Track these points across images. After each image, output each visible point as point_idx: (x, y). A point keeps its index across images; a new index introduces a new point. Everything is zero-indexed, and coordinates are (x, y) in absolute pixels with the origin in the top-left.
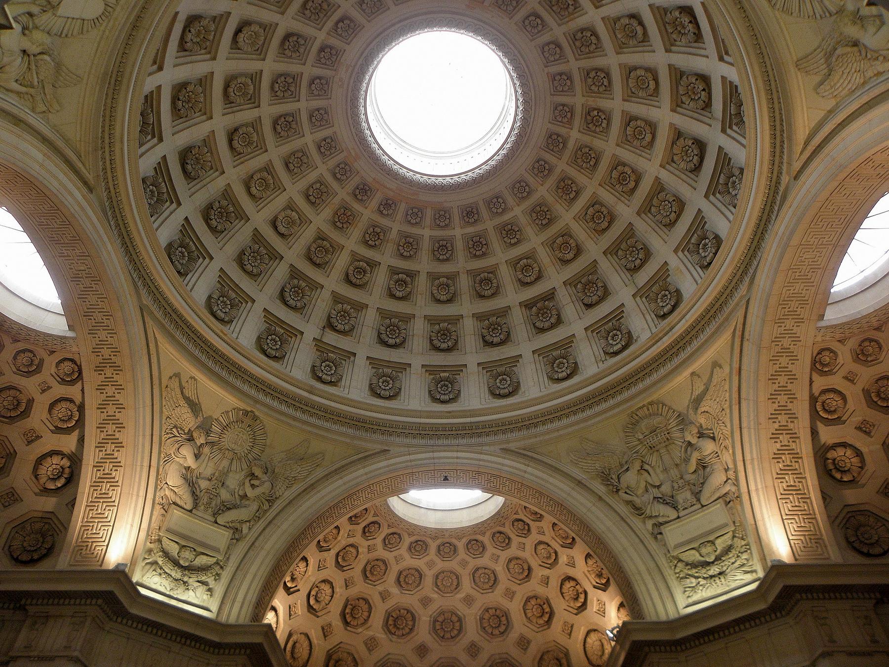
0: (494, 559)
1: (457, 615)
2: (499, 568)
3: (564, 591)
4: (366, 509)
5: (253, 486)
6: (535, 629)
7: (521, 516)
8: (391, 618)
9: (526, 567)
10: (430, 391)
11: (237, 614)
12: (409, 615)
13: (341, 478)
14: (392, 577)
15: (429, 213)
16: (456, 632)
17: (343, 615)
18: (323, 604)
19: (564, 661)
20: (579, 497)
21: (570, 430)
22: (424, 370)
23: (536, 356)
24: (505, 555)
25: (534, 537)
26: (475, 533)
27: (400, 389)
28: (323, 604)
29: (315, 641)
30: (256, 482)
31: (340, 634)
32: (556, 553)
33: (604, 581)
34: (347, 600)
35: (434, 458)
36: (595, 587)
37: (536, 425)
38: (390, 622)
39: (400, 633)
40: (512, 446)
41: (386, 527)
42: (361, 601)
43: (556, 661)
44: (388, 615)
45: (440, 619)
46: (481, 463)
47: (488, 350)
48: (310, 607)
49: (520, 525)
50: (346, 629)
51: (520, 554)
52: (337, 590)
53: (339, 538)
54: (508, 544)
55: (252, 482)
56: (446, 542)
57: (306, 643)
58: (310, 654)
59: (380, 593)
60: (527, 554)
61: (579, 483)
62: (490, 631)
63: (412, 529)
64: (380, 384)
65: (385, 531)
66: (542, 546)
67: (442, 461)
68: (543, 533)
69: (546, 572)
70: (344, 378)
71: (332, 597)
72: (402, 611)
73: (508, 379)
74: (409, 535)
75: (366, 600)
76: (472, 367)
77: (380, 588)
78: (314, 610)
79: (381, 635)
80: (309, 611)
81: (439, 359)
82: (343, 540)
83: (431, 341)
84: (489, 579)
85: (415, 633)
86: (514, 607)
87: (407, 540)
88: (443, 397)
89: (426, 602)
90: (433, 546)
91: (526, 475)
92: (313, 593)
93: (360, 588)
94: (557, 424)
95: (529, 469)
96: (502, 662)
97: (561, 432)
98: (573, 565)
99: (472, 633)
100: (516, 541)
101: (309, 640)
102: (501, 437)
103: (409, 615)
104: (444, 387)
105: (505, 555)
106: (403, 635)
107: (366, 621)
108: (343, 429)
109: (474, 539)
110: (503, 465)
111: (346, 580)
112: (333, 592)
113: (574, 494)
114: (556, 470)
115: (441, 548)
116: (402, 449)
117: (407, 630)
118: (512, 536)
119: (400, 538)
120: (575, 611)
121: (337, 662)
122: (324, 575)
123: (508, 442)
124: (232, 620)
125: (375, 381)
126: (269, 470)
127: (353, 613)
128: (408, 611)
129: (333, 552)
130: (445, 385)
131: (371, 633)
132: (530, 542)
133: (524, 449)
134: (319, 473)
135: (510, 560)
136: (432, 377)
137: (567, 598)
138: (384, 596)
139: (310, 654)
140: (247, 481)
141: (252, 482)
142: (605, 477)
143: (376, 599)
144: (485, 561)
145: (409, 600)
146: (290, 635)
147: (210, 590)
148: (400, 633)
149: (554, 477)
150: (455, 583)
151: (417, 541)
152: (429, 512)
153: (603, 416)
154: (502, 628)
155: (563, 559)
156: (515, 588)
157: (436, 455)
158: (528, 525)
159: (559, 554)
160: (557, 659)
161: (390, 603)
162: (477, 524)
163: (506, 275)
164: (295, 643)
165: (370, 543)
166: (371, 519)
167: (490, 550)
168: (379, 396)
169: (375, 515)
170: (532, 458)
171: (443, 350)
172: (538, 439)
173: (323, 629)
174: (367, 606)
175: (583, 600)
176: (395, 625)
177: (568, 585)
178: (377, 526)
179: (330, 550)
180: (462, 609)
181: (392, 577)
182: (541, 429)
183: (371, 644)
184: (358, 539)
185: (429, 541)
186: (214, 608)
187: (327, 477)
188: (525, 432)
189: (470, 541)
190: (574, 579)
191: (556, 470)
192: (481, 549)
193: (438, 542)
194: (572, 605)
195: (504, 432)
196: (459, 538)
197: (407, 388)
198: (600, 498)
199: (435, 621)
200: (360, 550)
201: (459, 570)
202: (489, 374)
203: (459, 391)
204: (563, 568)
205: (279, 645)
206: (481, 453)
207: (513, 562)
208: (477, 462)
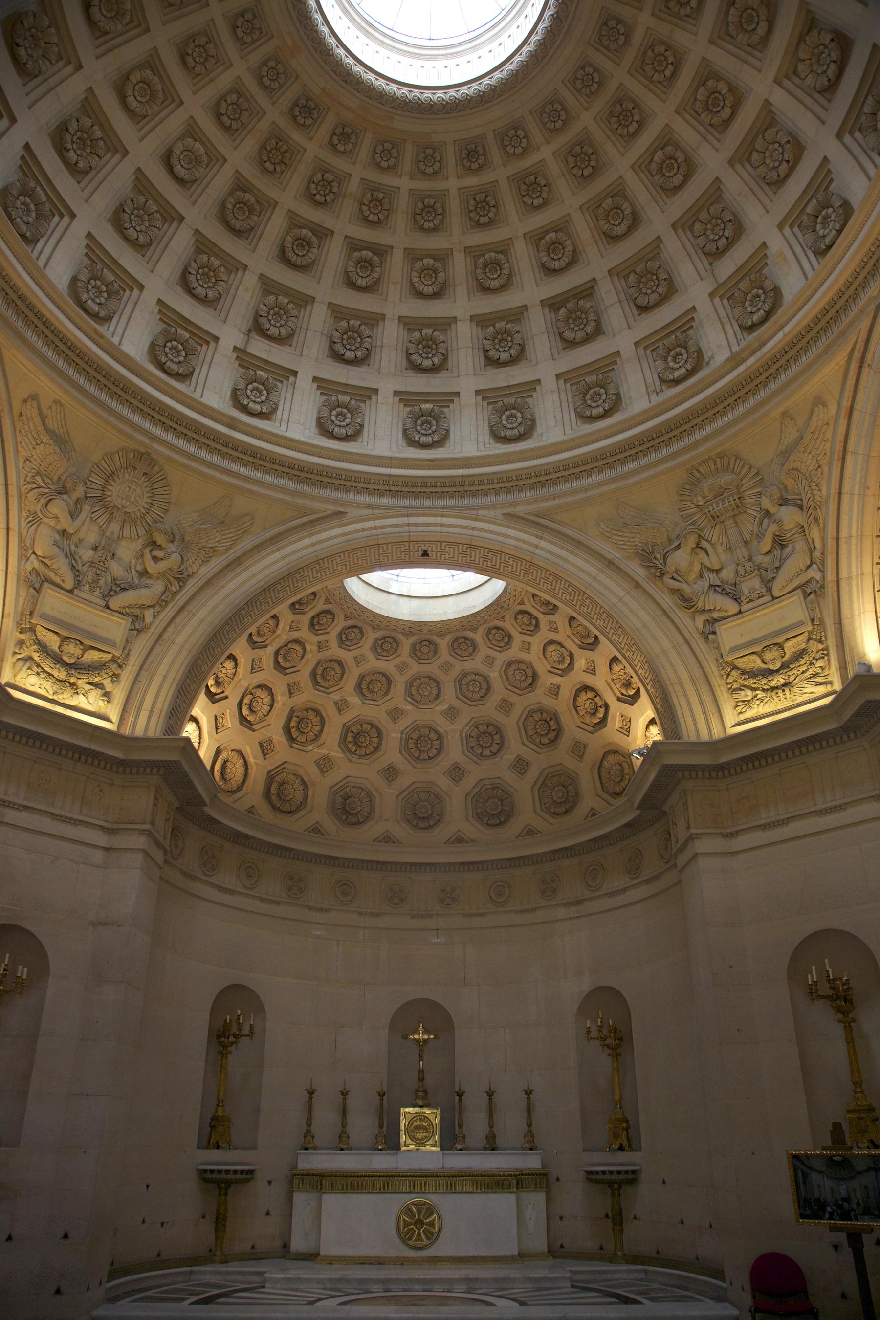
0: (489, 662)
1: (436, 732)
2: (494, 675)
3: (579, 704)
4: (314, 594)
5: (155, 559)
7: (528, 607)
8: (350, 734)
9: (530, 674)
10: (405, 431)
12: (374, 730)
13: (278, 550)
14: (350, 682)
15: (409, 151)
16: (434, 752)
17: (287, 729)
18: (260, 714)
20: (608, 582)
21: (604, 489)
22: (397, 399)
23: (561, 382)
24: (501, 658)
25: (544, 635)
26: (464, 628)
27: (362, 426)
28: (260, 714)
29: (251, 760)
30: (159, 554)
31: (283, 752)
32: (571, 656)
33: (632, 692)
34: (292, 711)
35: (408, 525)
36: (619, 699)
37: (555, 482)
38: (349, 739)
39: (363, 752)
40: (520, 510)
41: (342, 617)
42: (310, 712)
43: (561, 788)
44: (347, 729)
45: (415, 736)
46: (476, 533)
47: (492, 371)
48: (243, 719)
49: (526, 619)
50: (292, 747)
51: (523, 656)
52: (279, 698)
53: (279, 632)
54: (507, 643)
55: (155, 553)
56: (424, 638)
57: (239, 763)
59: (336, 703)
60: (534, 656)
61: (610, 564)
62: (479, 752)
63: (379, 622)
64: (333, 418)
65: (340, 623)
66: (552, 648)
67: (420, 528)
68: (556, 630)
69: (557, 680)
70: (280, 408)
71: (272, 706)
72: (365, 726)
73: (519, 415)
74: (373, 628)
75: (317, 712)
76: (468, 397)
79: (337, 754)
80: (241, 723)
81: (419, 383)
82: (283, 635)
83: (409, 355)
84: (480, 688)
85: (379, 754)
86: (510, 724)
87: (371, 636)
88: (424, 439)
89: (395, 714)
90: (406, 644)
91: (538, 551)
92: (246, 701)
93: (308, 695)
94: (585, 481)
95: (542, 543)
96: (493, 788)
97: (590, 493)
98: (593, 672)
99: (454, 753)
100: (518, 639)
102: (505, 498)
103: (374, 730)
104: (426, 422)
105: (501, 658)
106: (366, 754)
107: (317, 737)
108: (280, 482)
109: (460, 634)
110: (506, 536)
111: (289, 685)
112: (273, 700)
113: (602, 577)
114: (579, 544)
115: (417, 647)
116: (365, 512)
117: (371, 748)
118: (515, 634)
119: (362, 632)
121: (281, 784)
122: (259, 678)
123: (514, 504)
125: (325, 413)
126: (177, 538)
127: (300, 726)
128: (373, 726)
129: (271, 650)
130: (427, 422)
131: (325, 752)
132: (537, 641)
133: (538, 516)
134: (247, 543)
135: (509, 665)
136: (408, 409)
137: (581, 713)
138: (341, 706)
140: (147, 551)
141: (155, 553)
142: (646, 557)
143: (330, 711)
144: (476, 664)
145: (376, 712)
146: (218, 752)
148: (363, 752)
149: (576, 555)
150: (435, 692)
151: (385, 638)
152: (402, 600)
153: (652, 472)
154: (495, 748)
155: (581, 663)
156: (514, 698)
157: (412, 520)
158: (536, 619)
159: (576, 657)
161: (348, 716)
162: (467, 617)
163: (523, 257)
164: (225, 762)
165: (321, 638)
166: (321, 606)
167: (484, 650)
168: (331, 435)
169: (327, 601)
170: (547, 527)
171: (426, 370)
172: (557, 501)
173: (261, 745)
174: (318, 718)
175: (602, 716)
176: (356, 743)
177: (583, 697)
178: (329, 616)
179: (266, 646)
180: (443, 725)
181: (350, 682)
182: (563, 487)
183: (325, 764)
184: (304, 633)
185: (401, 637)
187: (258, 548)
188: (539, 492)
189: (457, 639)
190: (592, 689)
191: (579, 544)
192: (471, 649)
193: (413, 639)
194: (588, 720)
195: (509, 491)
196: (441, 635)
197: (372, 426)
198: (637, 585)
199: (409, 738)
200: (308, 647)
201: (439, 675)
202: (491, 407)
203: (448, 431)
204: (578, 676)
206: (476, 520)
207: (513, 667)
208: (469, 532)
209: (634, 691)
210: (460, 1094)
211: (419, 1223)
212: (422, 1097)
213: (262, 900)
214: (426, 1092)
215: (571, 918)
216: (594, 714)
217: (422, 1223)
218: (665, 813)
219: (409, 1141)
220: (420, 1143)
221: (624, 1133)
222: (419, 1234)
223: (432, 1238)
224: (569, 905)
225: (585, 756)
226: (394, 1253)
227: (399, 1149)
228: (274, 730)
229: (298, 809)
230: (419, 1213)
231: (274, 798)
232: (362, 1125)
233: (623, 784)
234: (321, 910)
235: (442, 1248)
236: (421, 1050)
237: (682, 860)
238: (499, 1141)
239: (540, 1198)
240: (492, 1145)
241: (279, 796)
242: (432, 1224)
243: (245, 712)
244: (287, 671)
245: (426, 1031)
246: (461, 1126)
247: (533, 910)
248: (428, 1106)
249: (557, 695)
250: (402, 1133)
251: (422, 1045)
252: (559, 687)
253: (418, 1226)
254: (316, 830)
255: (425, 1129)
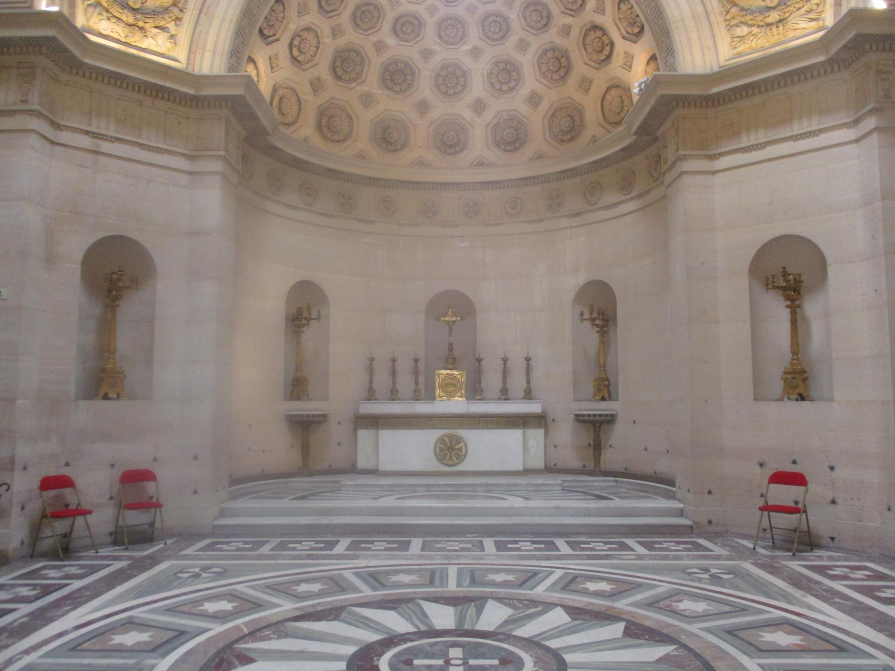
6: (549, 85)
9: (545, 14)
11: (210, 62)
14: (386, 27)
16: (460, 88)
19: (577, 118)
28: (308, 56)
33: (636, 30)
58: (300, 110)
62: (498, 87)
69: (569, 20)
71: (318, 48)
77: (374, 38)
78: (299, 62)
96: (510, 119)
101: (297, 94)
111: (332, 28)
112: (319, 42)
120: (597, 66)
121: (331, 118)
124: (206, 71)
137: (590, 51)
139: (300, 110)
146: (275, 90)
147: (172, 37)
160: (570, 116)
164: (281, 99)
173: (312, 84)
186: (181, 54)
205: (263, 99)
209: (638, 30)
210: (479, 360)
211: (451, 448)
212: (451, 361)
213: (321, 214)
214: (454, 359)
215: (572, 227)
216: (601, 51)
217: (453, 449)
218: (657, 138)
219: (442, 394)
220: (451, 394)
221: (605, 388)
222: (451, 457)
223: (461, 458)
224: (570, 216)
225: (591, 90)
226: (432, 468)
227: (434, 399)
228: (322, 70)
229: (345, 139)
230: (451, 442)
231: (325, 129)
232: (405, 383)
233: (622, 115)
234: (368, 222)
235: (468, 465)
236: (451, 329)
237: (668, 179)
238: (510, 394)
239: (541, 432)
240: (505, 395)
241: (329, 128)
242: (460, 449)
243: (296, 53)
244: (330, 15)
245: (454, 314)
246: (480, 383)
247: (541, 221)
248: (456, 369)
249: (568, 34)
250: (437, 388)
251: (450, 325)
252: (570, 27)
253: (450, 451)
254: (361, 156)
255: (454, 385)
